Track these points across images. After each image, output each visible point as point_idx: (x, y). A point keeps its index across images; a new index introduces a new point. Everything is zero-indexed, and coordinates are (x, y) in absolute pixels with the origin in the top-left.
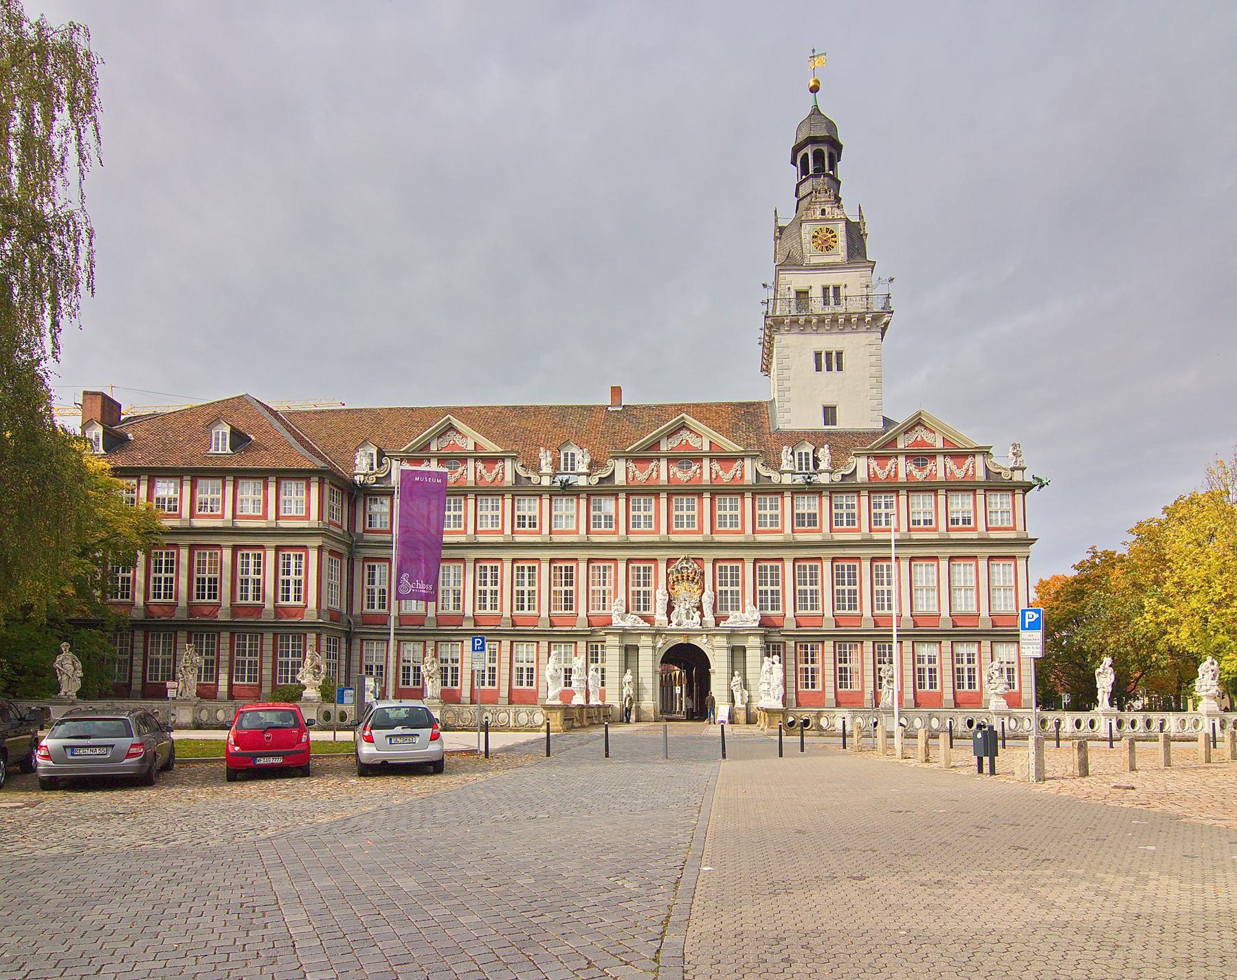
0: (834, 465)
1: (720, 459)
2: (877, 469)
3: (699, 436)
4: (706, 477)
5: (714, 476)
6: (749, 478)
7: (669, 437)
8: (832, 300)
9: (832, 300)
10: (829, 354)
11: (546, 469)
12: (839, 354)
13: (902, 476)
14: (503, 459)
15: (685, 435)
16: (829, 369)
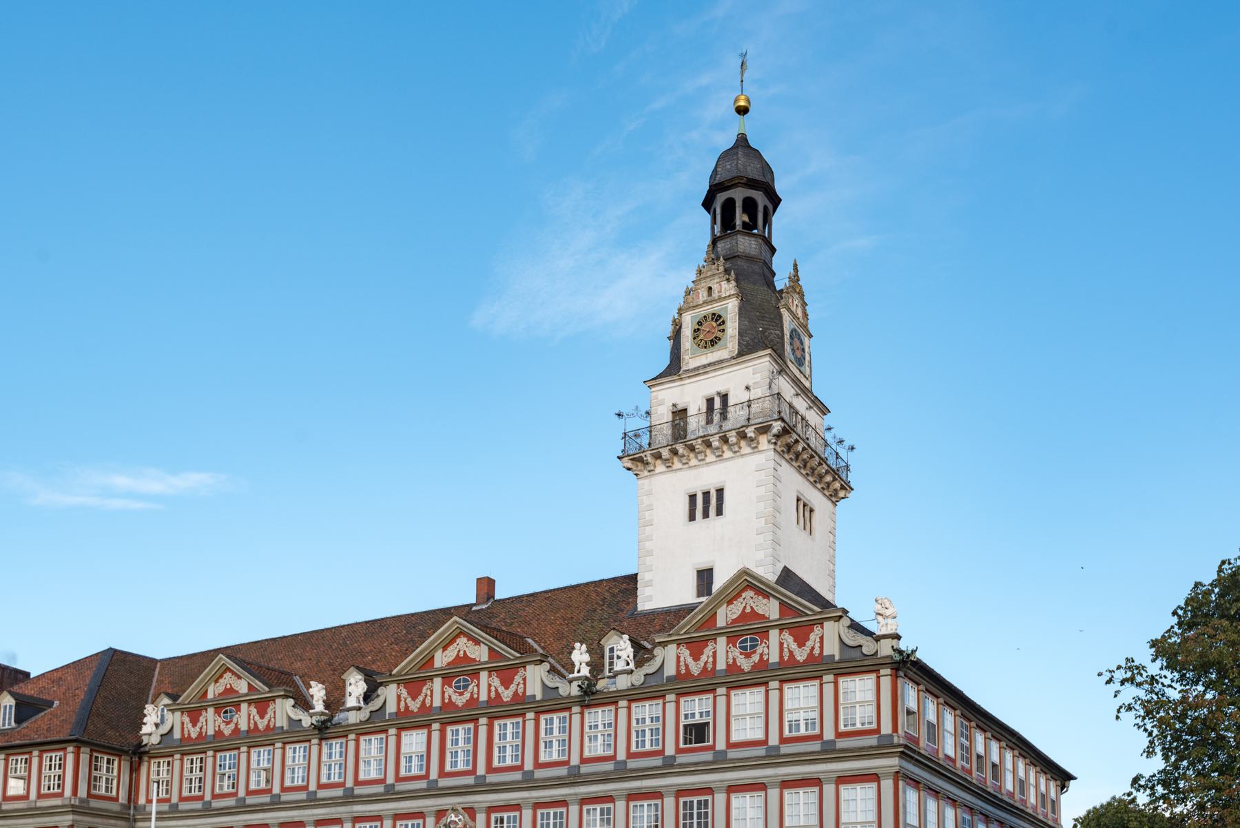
0: (639, 663)
1: (498, 670)
2: (690, 660)
3: (477, 642)
4: (483, 697)
5: (493, 695)
6: (534, 690)
7: (445, 648)
8: (716, 417)
9: (716, 417)
10: (706, 495)
11: (319, 707)
12: (720, 492)
13: (721, 665)
14: (273, 699)
15: (462, 641)
16: (706, 515)
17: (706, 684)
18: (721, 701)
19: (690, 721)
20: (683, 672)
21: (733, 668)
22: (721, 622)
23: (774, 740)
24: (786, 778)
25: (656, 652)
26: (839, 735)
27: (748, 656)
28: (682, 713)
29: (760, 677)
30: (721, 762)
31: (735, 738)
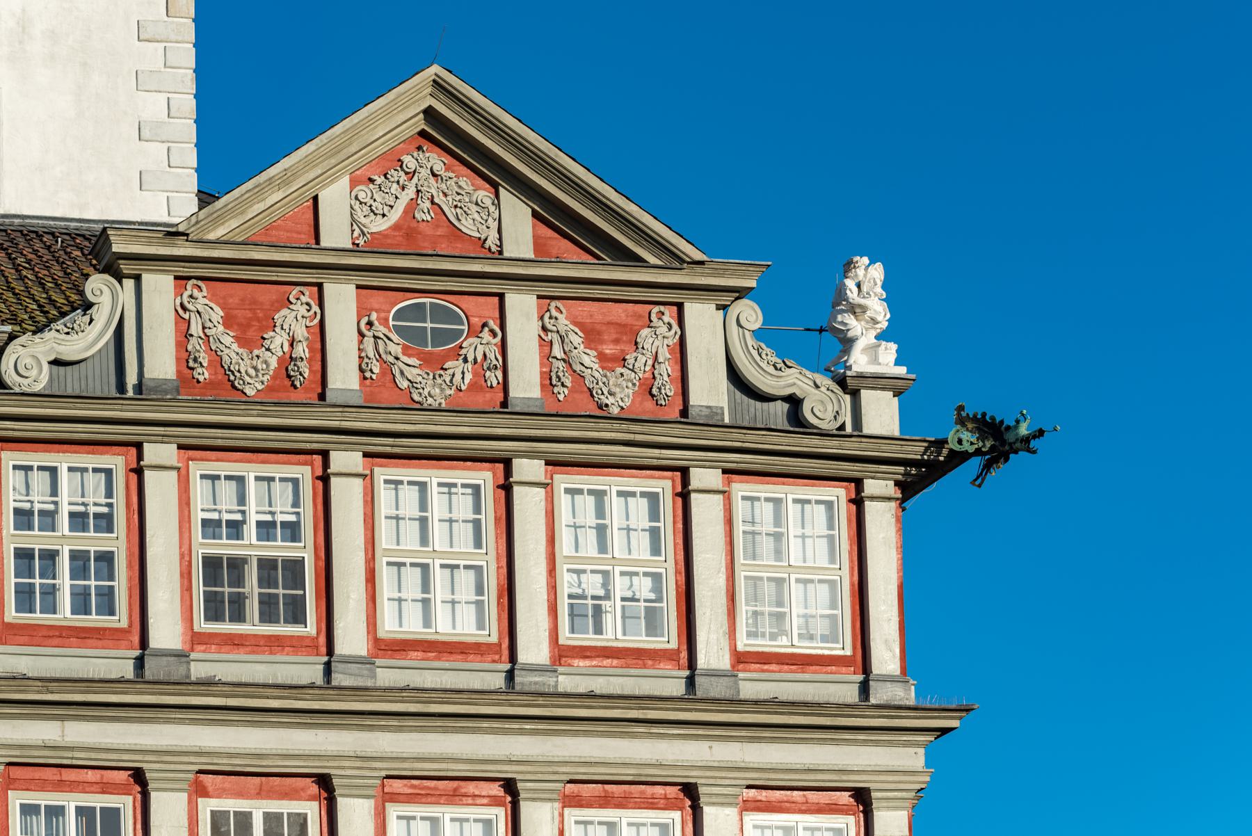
13: (344, 377)
17: (299, 426)
18: (347, 495)
19: (224, 547)
20: (203, 374)
21: (379, 384)
22: (336, 233)
23: (534, 648)
24: (582, 772)
25: (98, 286)
26: (741, 659)
27: (434, 363)
28: (199, 515)
29: (486, 440)
30: (331, 700)
31: (389, 626)
